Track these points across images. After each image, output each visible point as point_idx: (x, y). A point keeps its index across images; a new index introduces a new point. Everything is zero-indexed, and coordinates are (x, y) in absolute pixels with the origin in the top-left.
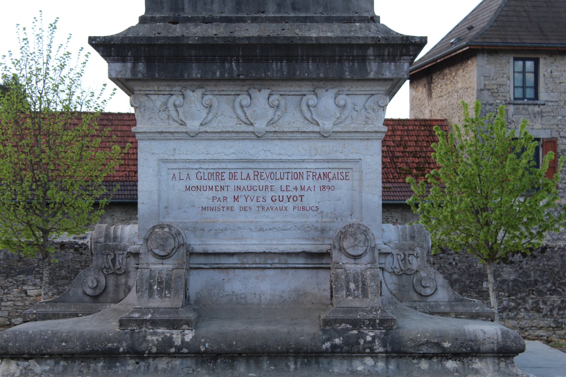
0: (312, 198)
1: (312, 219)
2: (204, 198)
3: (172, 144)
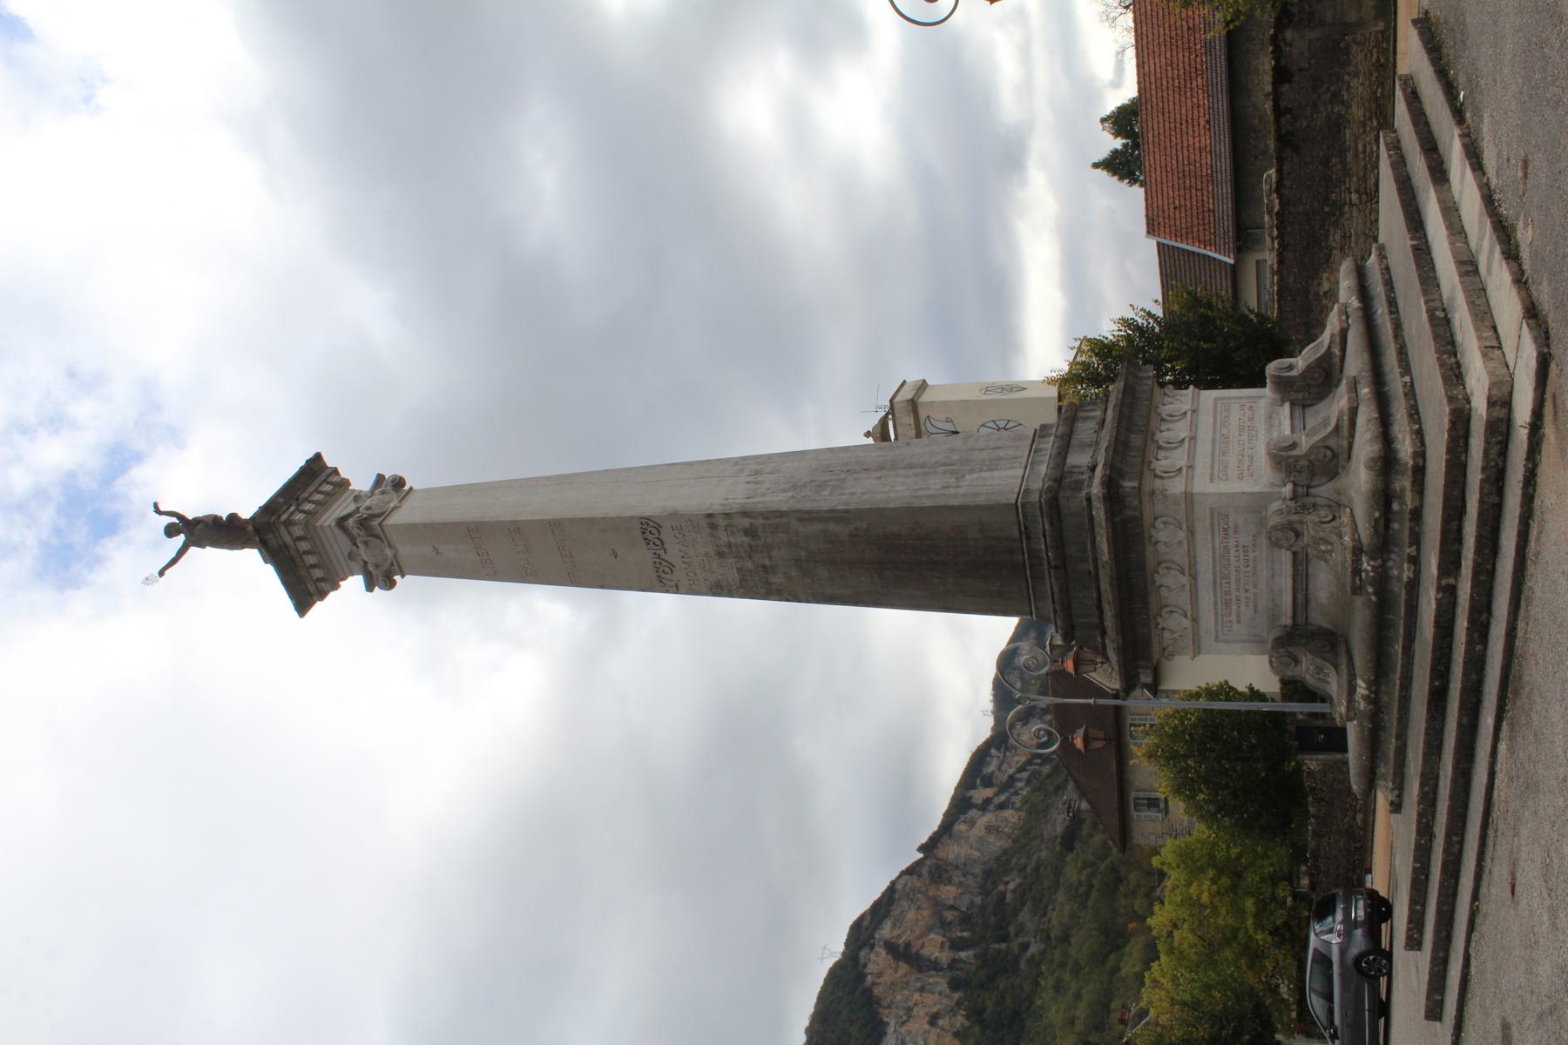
0: (1245, 539)
3: (1202, 633)
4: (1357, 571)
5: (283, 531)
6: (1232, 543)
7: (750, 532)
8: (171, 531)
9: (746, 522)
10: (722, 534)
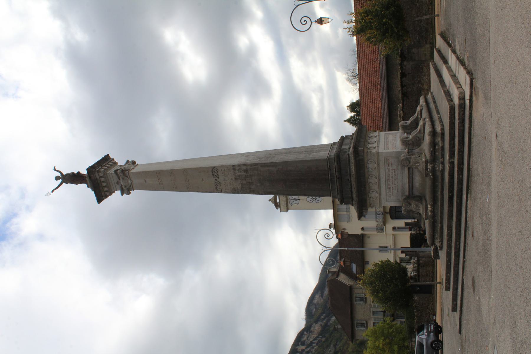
0: (394, 167)
1: (400, 167)
2: (395, 191)
3: (382, 199)
4: (427, 169)
5: (97, 174)
6: (390, 169)
7: (246, 171)
8: (57, 178)
9: (244, 168)
10: (237, 172)
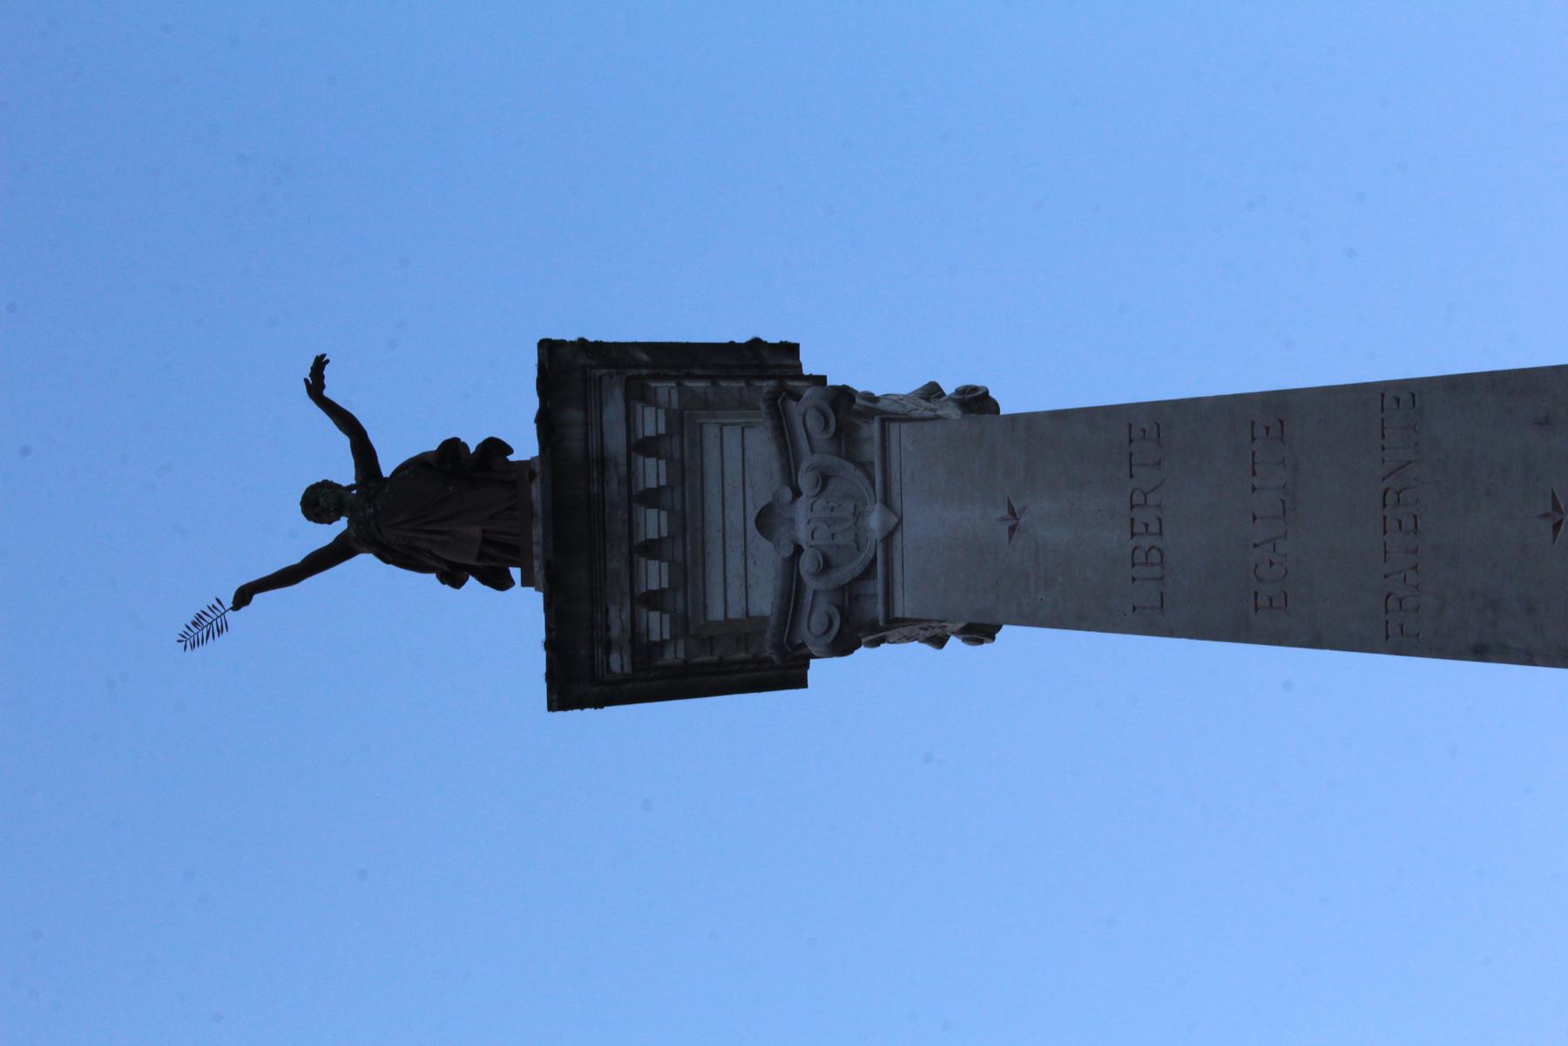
5: (614, 412)
